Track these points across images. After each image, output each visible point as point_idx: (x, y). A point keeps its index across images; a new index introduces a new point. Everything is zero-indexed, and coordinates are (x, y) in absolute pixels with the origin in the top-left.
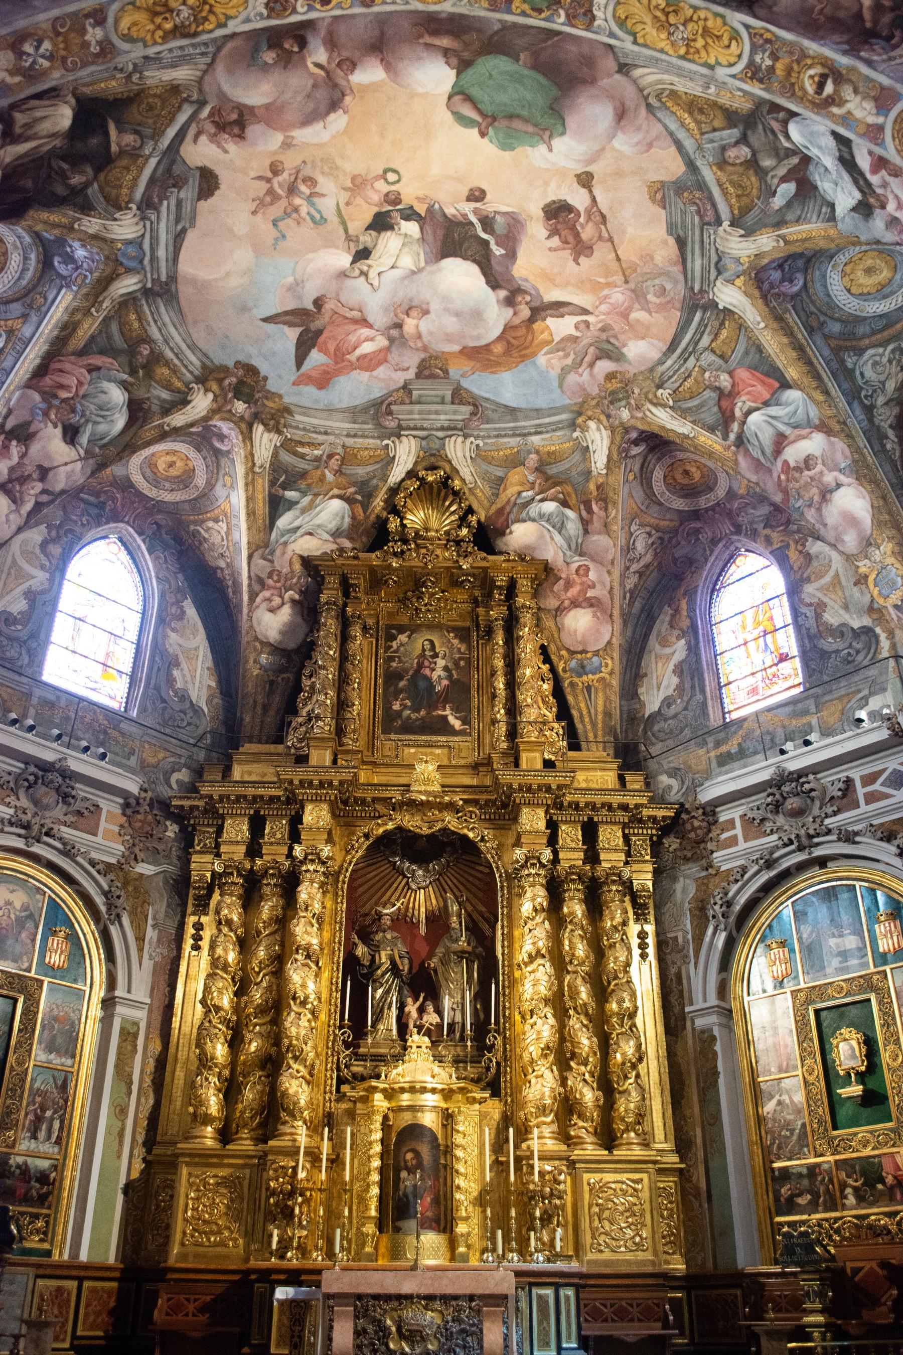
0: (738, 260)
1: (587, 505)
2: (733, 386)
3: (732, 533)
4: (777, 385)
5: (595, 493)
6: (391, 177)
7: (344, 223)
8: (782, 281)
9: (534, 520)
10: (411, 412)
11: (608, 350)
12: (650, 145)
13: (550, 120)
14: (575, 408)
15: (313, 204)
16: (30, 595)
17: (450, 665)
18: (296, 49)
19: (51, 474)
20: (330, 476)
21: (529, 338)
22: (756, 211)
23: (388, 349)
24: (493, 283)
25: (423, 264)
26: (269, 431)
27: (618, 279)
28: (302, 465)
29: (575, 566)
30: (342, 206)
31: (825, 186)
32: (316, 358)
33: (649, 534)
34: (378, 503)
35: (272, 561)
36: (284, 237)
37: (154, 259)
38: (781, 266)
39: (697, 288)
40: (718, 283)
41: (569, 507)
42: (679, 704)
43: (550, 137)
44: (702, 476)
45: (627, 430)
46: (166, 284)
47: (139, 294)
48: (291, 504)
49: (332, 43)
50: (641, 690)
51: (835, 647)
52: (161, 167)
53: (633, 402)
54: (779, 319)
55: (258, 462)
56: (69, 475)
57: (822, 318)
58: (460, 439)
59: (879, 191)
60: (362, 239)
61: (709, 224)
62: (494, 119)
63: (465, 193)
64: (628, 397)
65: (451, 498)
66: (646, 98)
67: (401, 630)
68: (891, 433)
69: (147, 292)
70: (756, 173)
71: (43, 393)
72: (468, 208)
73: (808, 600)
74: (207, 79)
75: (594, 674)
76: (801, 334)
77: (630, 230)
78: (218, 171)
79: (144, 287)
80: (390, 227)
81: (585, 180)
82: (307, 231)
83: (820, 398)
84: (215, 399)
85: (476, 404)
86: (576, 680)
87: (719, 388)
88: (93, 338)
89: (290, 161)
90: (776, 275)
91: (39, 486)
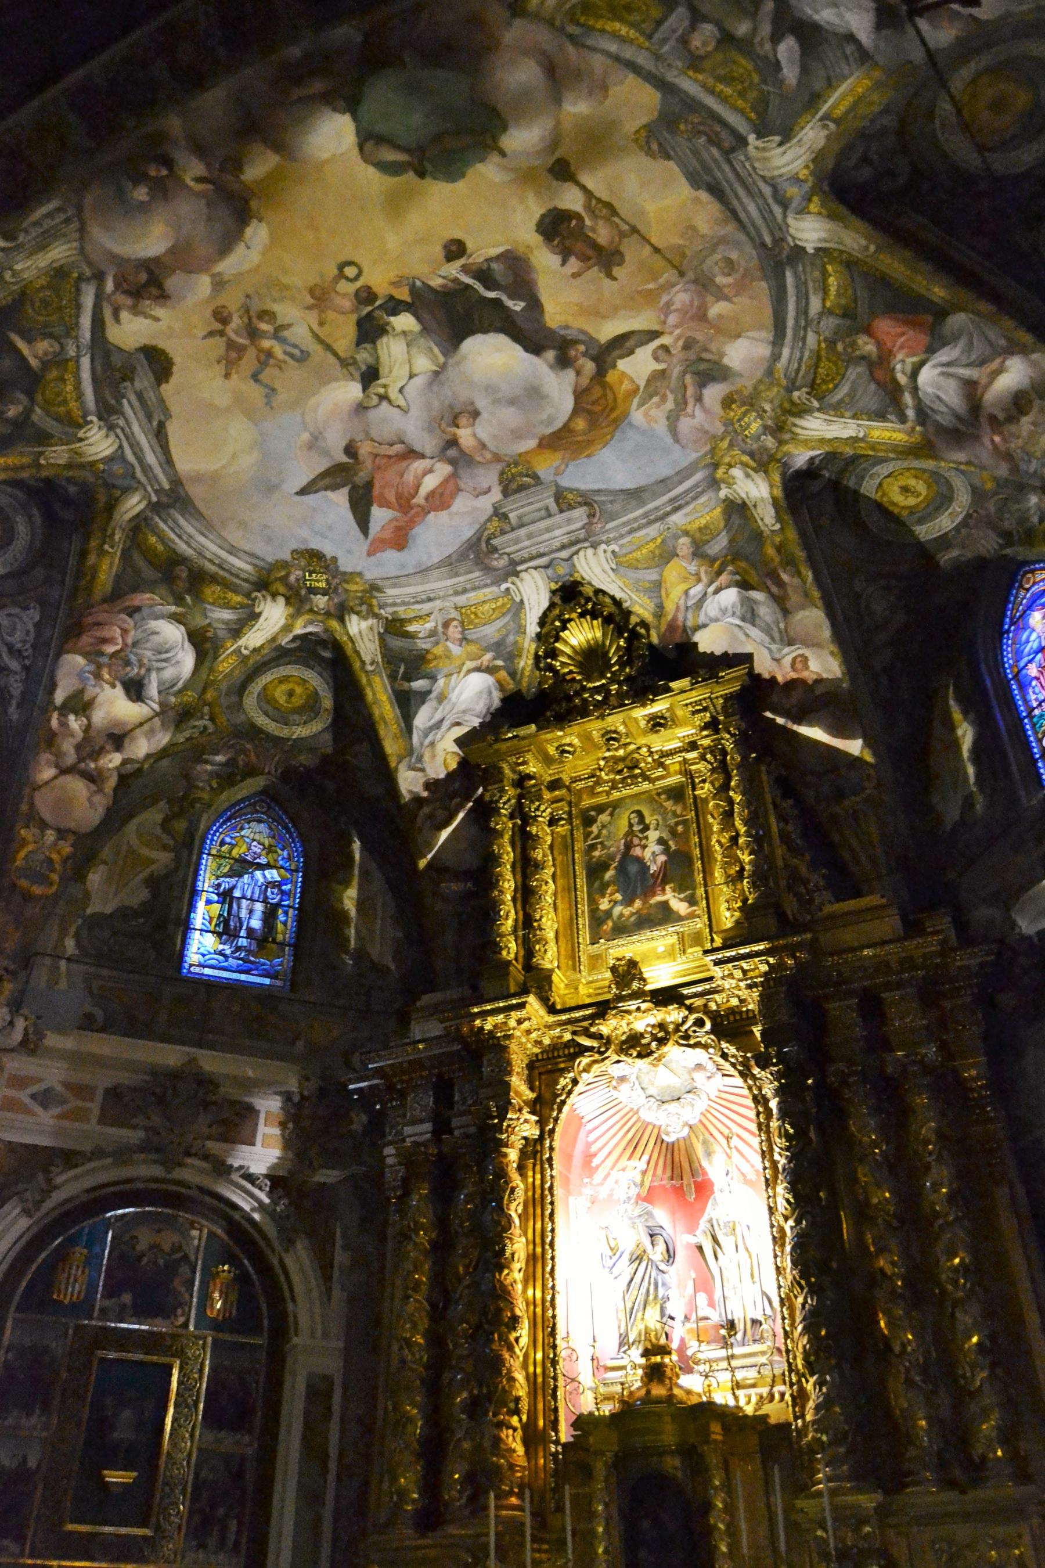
0: (795, 179)
5: (777, 559)
7: (328, 348)
9: (717, 620)
10: (517, 541)
11: (709, 371)
14: (708, 460)
15: (283, 341)
16: (153, 883)
17: (665, 835)
18: (164, 172)
20: (455, 649)
21: (610, 396)
22: (774, 102)
23: (454, 475)
24: (534, 348)
25: (442, 359)
26: (365, 618)
27: (670, 275)
29: (787, 661)
32: (380, 516)
35: (423, 770)
36: (273, 390)
37: (146, 469)
39: (768, 240)
40: (790, 221)
41: (753, 588)
43: (495, 139)
44: (929, 487)
48: (423, 696)
49: (200, 150)
50: (935, 799)
55: (368, 662)
58: (590, 551)
60: (358, 357)
61: (733, 150)
63: (438, 251)
66: (562, 30)
69: (156, 507)
71: (85, 655)
74: (89, 248)
77: (650, 207)
78: (162, 344)
79: (150, 502)
80: (382, 330)
82: (295, 373)
85: (586, 500)
86: (837, 809)
87: (863, 358)
88: (118, 578)
89: (232, 300)
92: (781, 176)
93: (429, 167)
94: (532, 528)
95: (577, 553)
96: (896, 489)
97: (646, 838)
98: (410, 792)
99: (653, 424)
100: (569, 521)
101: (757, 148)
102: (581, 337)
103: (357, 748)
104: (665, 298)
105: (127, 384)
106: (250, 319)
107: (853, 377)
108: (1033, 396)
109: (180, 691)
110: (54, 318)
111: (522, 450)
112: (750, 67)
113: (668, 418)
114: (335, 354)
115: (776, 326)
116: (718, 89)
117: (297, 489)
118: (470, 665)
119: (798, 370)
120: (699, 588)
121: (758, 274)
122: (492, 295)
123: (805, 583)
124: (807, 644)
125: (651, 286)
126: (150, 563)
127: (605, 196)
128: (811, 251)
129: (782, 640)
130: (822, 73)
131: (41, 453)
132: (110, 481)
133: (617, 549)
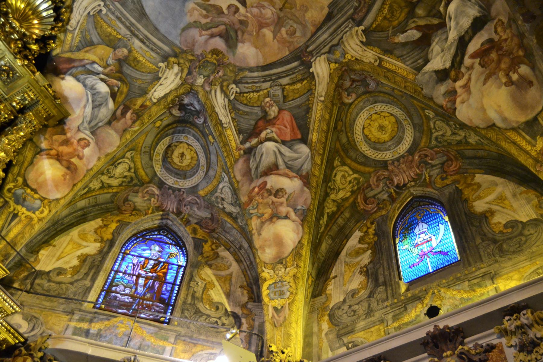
0: (344, 54)
4: (299, 136)
5: (137, 107)
8: (346, 90)
9: (85, 86)
11: (231, 37)
14: (177, 51)
29: (82, 135)
31: (436, 47)
33: (130, 169)
38: (353, 81)
39: (310, 49)
40: (323, 57)
41: (114, 100)
42: (67, 278)
44: (188, 166)
45: (191, 91)
51: (208, 312)
53: (212, 78)
54: (333, 104)
57: (343, 128)
59: (463, 70)
61: (354, 20)
64: (213, 72)
75: (28, 210)
83: (319, 162)
86: (12, 203)
90: (347, 83)
92: (345, 46)
99: (189, 14)
101: (357, 31)
104: (266, 4)
107: (254, 111)
108: (286, 196)
112: (400, 20)
113: (195, 22)
115: (268, 65)
116: (385, 6)
119: (248, 83)
121: (292, 48)
123: (130, 127)
124: (97, 143)
128: (311, 70)
130: (405, 53)
133: (104, 12)
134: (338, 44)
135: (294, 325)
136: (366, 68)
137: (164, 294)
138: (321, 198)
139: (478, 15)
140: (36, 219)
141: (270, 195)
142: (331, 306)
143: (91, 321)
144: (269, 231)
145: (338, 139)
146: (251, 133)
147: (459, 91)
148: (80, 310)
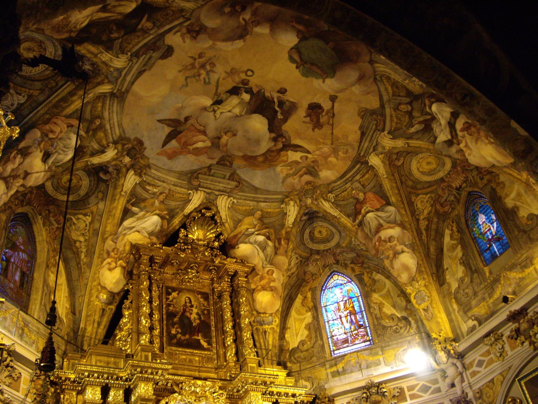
0: (384, 148)
1: (279, 240)
2: (364, 199)
3: (334, 264)
4: (384, 203)
5: (284, 235)
6: (249, 73)
8: (396, 159)
9: (251, 243)
10: (207, 180)
11: (312, 171)
12: (368, 93)
13: (329, 70)
14: (287, 194)
17: (200, 312)
18: (239, 10)
19: (29, 176)
20: (157, 203)
21: (277, 157)
22: (401, 131)
23: (209, 148)
24: (271, 130)
25: (243, 113)
26: (136, 174)
27: (329, 142)
28: (146, 195)
29: (267, 269)
30: (221, 79)
32: (174, 143)
33: (297, 258)
34: (176, 222)
39: (362, 154)
40: (372, 155)
43: (327, 77)
44: (327, 235)
46: (123, 93)
47: (108, 95)
48: (134, 214)
49: (254, 13)
51: (389, 325)
52: (153, 40)
53: (315, 196)
55: (124, 191)
56: (37, 178)
57: (406, 178)
58: (226, 197)
59: (460, 138)
60: (222, 95)
61: (379, 130)
62: (306, 63)
63: (278, 88)
64: (314, 193)
65: (213, 225)
66: (375, 75)
67: (174, 290)
68: (424, 232)
69: (112, 95)
70: (409, 117)
71: (42, 133)
72: (275, 95)
73: (375, 301)
75: (269, 325)
76: (399, 184)
81: (333, 99)
83: (404, 213)
84: (117, 154)
85: (240, 181)
86: (259, 327)
89: (209, 54)
90: (395, 157)
91: (21, 182)
93: (301, 67)
94: (215, 178)
95: (222, 195)
96: (318, 230)
97: (192, 310)
98: (107, 250)
100: (228, 184)
102: (287, 138)
103: (81, 216)
104: (321, 146)
105: (152, 52)
106: (207, 62)
108: (396, 239)
109: (58, 167)
110: (162, 20)
111: (236, 154)
113: (287, 175)
114: (217, 90)
117: (158, 119)
118: (157, 212)
119: (337, 189)
120: (253, 230)
121: (351, 159)
122: (277, 109)
123: (288, 248)
124: (277, 268)
125: (321, 140)
126: (91, 111)
127: (335, 113)
129: (269, 262)
130: (420, 136)
131: (102, 53)
132: (109, 76)
134: (377, 145)
135: (438, 315)
136: (401, 150)
137: (360, 321)
138: (416, 226)
139: (452, 111)
140: (275, 327)
141: (387, 243)
142: (453, 291)
143: (336, 365)
144: (397, 264)
145: (407, 186)
146: (355, 213)
147: (464, 149)
148: (327, 361)
